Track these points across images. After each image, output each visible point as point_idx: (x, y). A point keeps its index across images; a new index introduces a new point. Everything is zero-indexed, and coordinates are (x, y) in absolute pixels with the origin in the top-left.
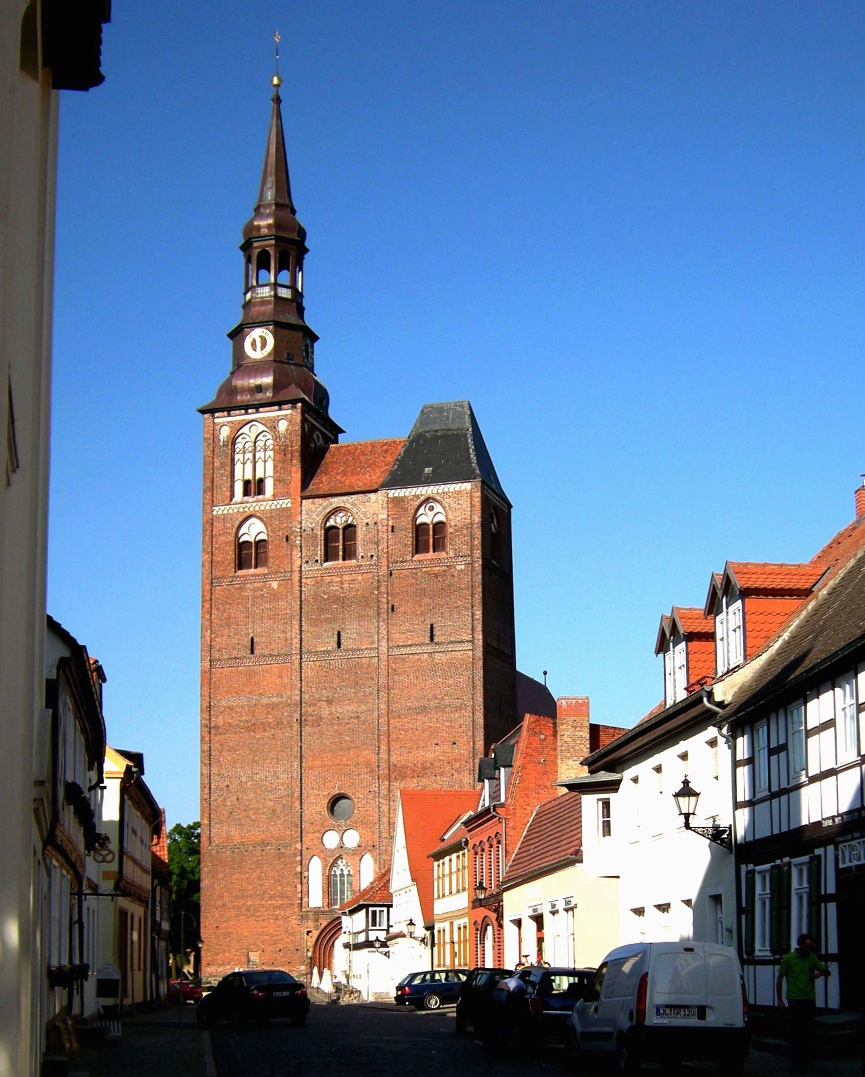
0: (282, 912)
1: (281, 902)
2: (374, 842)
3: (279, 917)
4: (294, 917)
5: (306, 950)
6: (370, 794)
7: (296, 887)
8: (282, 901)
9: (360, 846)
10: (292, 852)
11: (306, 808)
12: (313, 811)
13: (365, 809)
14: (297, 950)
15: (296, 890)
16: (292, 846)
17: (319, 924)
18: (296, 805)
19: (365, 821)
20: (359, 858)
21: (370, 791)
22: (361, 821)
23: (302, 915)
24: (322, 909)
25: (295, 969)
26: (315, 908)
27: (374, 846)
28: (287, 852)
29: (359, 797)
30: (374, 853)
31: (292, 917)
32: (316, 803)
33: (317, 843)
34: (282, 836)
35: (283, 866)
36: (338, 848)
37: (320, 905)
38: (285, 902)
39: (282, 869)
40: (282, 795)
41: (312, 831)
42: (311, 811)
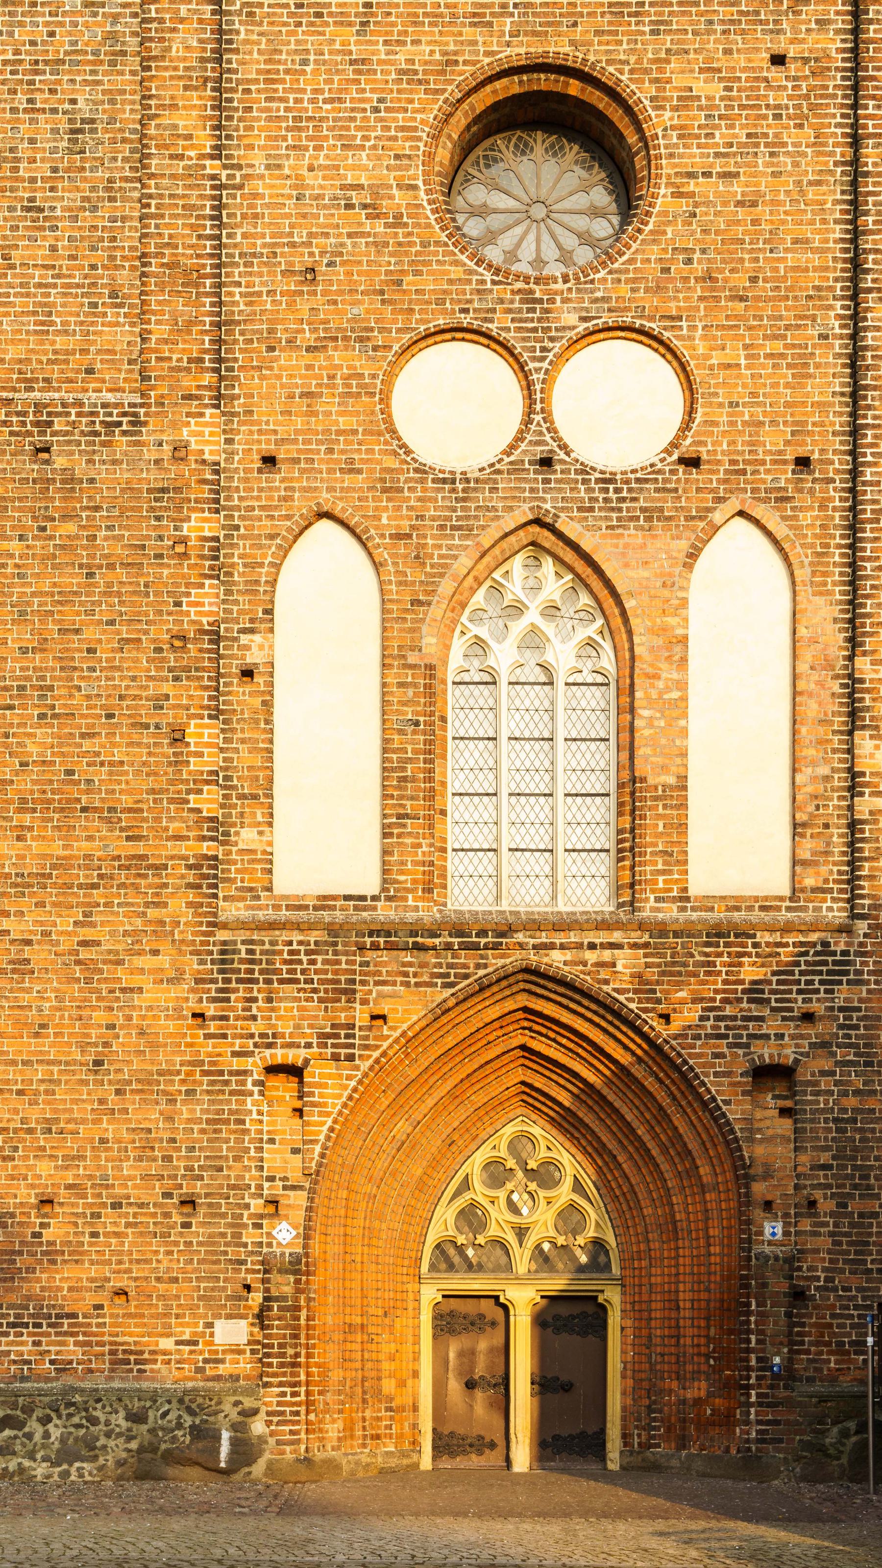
0: (65, 924)
1: (57, 849)
2: (799, 431)
3: (37, 955)
4: (164, 961)
5: (256, 1205)
6: (775, 73)
7: (178, 737)
8: (66, 831)
9: (693, 462)
10: (153, 477)
11: (258, 160)
12: (314, 180)
13: (737, 189)
14: (189, 1202)
15: (179, 763)
16: (147, 435)
17: (361, 1016)
18: (183, 121)
19: (741, 280)
20: (683, 545)
21: (778, 60)
22: (709, 277)
23: (227, 949)
24: (385, 912)
25: (166, 1344)
26: (325, 902)
27: (803, 462)
28: (101, 472)
29: (687, 99)
30: (806, 518)
31: (140, 962)
32: (341, 127)
33: (343, 422)
34: (60, 358)
35: (74, 580)
36: (516, 468)
37: (370, 885)
38: (82, 847)
39: (65, 598)
40: (62, 44)
41: (308, 337)
42: (300, 185)
